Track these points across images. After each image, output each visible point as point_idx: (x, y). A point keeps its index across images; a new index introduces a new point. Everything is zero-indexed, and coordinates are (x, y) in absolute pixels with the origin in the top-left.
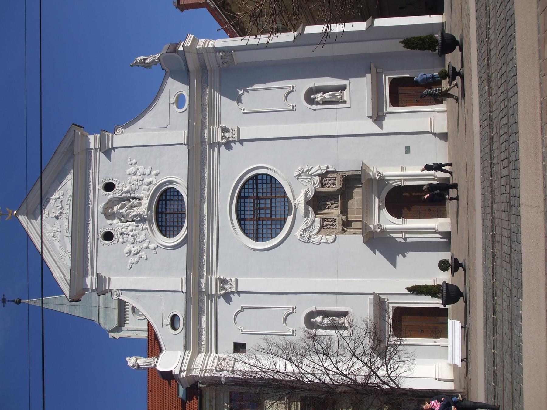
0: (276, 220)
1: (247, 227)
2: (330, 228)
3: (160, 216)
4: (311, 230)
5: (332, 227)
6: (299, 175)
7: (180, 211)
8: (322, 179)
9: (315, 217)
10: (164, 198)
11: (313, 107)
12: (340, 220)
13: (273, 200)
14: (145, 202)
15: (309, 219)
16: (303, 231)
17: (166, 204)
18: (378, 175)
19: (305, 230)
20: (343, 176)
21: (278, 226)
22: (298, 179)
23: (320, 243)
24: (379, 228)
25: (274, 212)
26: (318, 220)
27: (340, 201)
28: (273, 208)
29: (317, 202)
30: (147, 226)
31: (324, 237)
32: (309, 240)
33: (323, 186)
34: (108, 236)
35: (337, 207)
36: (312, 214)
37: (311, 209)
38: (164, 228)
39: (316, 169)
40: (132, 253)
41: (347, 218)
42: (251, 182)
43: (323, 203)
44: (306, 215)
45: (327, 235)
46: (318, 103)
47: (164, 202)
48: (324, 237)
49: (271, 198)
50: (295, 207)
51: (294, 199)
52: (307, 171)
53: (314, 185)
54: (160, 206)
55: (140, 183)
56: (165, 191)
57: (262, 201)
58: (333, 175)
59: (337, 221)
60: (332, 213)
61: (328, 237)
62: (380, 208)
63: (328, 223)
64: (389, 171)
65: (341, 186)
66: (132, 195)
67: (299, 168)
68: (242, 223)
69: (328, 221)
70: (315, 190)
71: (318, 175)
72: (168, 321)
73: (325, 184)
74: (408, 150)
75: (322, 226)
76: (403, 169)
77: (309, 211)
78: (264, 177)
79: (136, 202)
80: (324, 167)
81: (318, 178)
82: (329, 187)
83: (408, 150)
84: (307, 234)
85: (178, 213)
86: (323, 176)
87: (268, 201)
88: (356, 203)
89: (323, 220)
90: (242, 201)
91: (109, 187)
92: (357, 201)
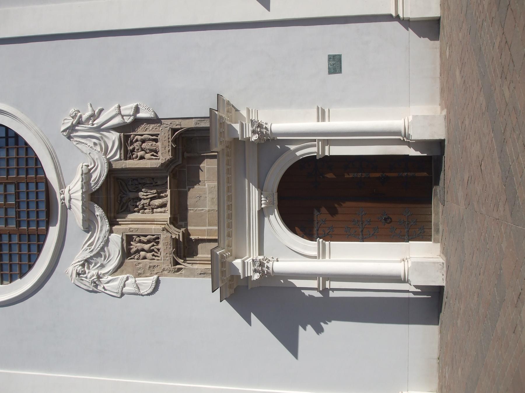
2: (145, 258)
4: (100, 260)
5: (149, 255)
6: (72, 129)
8: (127, 137)
9: (111, 232)
12: (169, 240)
15: (97, 235)
16: (83, 265)
18: (254, 132)
19: (87, 262)
20: (174, 131)
22: (69, 137)
23: (122, 294)
24: (255, 271)
26: (116, 239)
27: (168, 192)
31: (131, 280)
32: (96, 286)
33: (128, 155)
35: (164, 205)
36: (103, 225)
37: (99, 212)
39: (109, 115)
41: (186, 235)
43: (132, 195)
44: (89, 225)
45: (139, 275)
50: (64, 206)
51: (62, 186)
52: (88, 119)
53: (106, 154)
58: (151, 129)
59: (161, 241)
60: (152, 222)
61: (140, 280)
62: (262, 214)
63: (140, 246)
64: (282, 122)
65: (169, 156)
67: (72, 111)
69: (140, 242)
70: (110, 164)
71: (117, 128)
73: (133, 150)
74: (335, 64)
75: (127, 253)
76: (322, 115)
77: (95, 217)
80: (128, 109)
81: (114, 137)
82: (142, 158)
83: (335, 64)
84: (92, 272)
86: (127, 130)
88: (208, 197)
89: (129, 239)
92: (210, 192)
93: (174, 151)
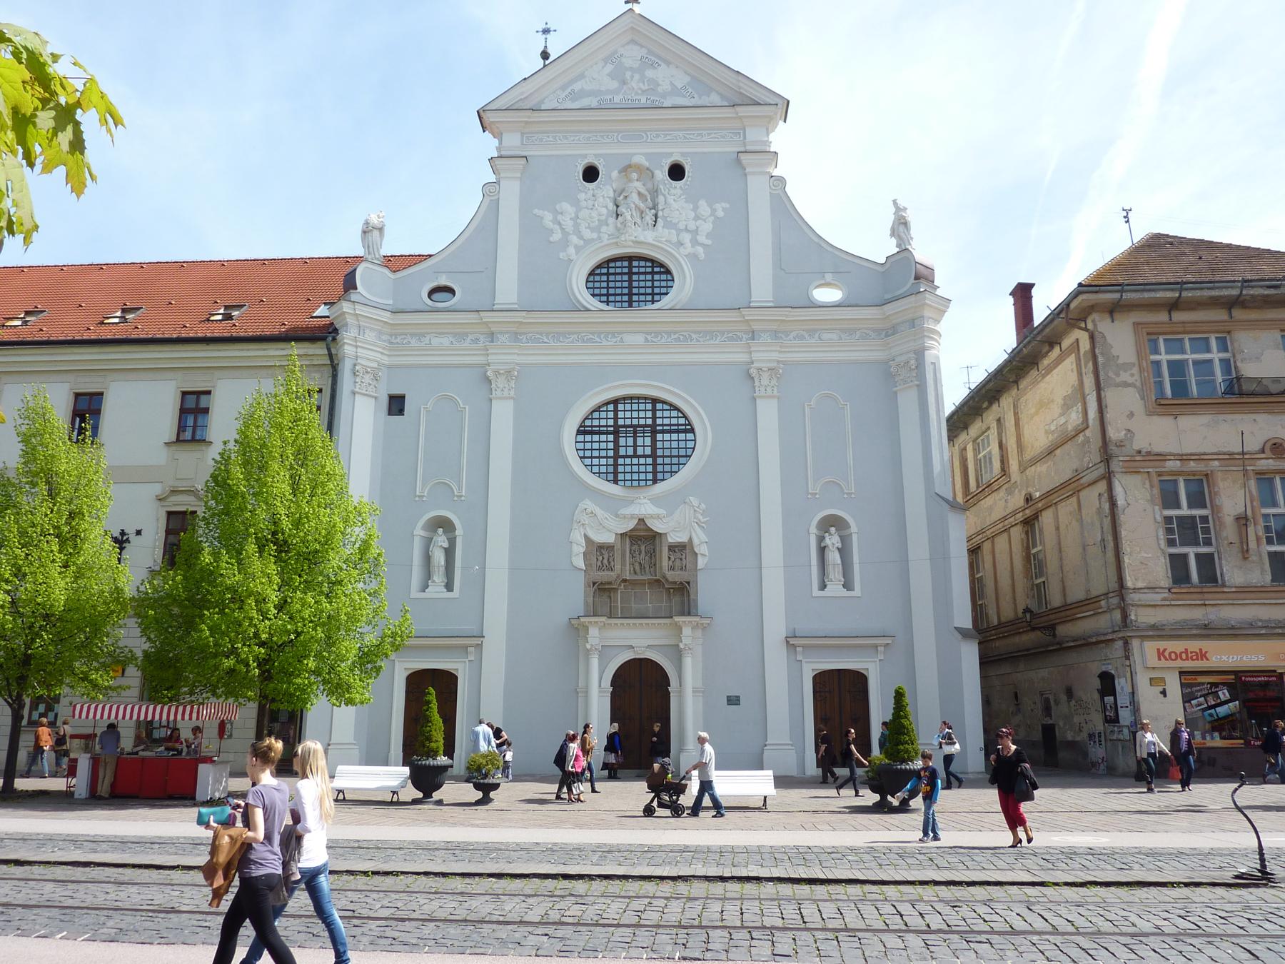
0: (616, 465)
1: (603, 415)
3: (626, 264)
7: (635, 298)
10: (656, 269)
11: (813, 530)
13: (649, 460)
14: (648, 236)
17: (645, 273)
21: (603, 469)
25: (628, 461)
26: (609, 538)
28: (635, 461)
29: (643, 538)
30: (606, 242)
33: (672, 548)
34: (591, 174)
38: (604, 271)
40: (559, 217)
42: (682, 421)
46: (821, 539)
47: (649, 270)
48: (582, 550)
49: (654, 456)
54: (642, 263)
55: (681, 226)
56: (668, 272)
57: (648, 441)
66: (660, 214)
68: (611, 407)
71: (690, 539)
72: (443, 281)
74: (733, 701)
75: (602, 547)
78: (690, 444)
79: (651, 222)
83: (733, 701)
85: (630, 294)
87: (648, 451)
89: (610, 548)
90: (649, 407)
91: (677, 172)
93: (675, 583)
